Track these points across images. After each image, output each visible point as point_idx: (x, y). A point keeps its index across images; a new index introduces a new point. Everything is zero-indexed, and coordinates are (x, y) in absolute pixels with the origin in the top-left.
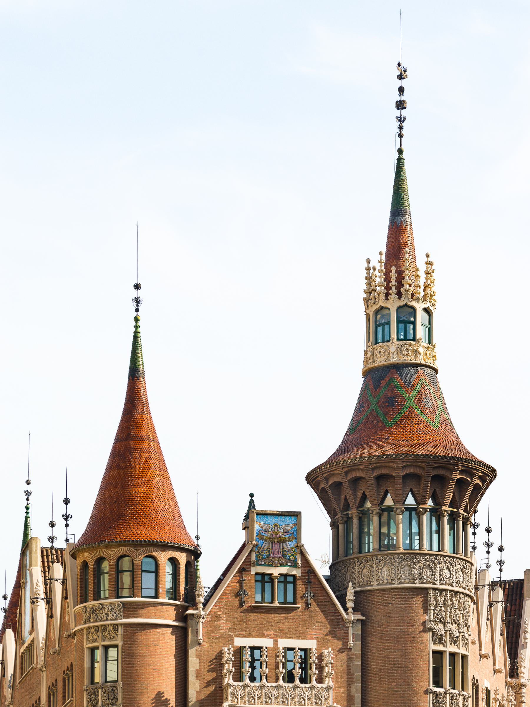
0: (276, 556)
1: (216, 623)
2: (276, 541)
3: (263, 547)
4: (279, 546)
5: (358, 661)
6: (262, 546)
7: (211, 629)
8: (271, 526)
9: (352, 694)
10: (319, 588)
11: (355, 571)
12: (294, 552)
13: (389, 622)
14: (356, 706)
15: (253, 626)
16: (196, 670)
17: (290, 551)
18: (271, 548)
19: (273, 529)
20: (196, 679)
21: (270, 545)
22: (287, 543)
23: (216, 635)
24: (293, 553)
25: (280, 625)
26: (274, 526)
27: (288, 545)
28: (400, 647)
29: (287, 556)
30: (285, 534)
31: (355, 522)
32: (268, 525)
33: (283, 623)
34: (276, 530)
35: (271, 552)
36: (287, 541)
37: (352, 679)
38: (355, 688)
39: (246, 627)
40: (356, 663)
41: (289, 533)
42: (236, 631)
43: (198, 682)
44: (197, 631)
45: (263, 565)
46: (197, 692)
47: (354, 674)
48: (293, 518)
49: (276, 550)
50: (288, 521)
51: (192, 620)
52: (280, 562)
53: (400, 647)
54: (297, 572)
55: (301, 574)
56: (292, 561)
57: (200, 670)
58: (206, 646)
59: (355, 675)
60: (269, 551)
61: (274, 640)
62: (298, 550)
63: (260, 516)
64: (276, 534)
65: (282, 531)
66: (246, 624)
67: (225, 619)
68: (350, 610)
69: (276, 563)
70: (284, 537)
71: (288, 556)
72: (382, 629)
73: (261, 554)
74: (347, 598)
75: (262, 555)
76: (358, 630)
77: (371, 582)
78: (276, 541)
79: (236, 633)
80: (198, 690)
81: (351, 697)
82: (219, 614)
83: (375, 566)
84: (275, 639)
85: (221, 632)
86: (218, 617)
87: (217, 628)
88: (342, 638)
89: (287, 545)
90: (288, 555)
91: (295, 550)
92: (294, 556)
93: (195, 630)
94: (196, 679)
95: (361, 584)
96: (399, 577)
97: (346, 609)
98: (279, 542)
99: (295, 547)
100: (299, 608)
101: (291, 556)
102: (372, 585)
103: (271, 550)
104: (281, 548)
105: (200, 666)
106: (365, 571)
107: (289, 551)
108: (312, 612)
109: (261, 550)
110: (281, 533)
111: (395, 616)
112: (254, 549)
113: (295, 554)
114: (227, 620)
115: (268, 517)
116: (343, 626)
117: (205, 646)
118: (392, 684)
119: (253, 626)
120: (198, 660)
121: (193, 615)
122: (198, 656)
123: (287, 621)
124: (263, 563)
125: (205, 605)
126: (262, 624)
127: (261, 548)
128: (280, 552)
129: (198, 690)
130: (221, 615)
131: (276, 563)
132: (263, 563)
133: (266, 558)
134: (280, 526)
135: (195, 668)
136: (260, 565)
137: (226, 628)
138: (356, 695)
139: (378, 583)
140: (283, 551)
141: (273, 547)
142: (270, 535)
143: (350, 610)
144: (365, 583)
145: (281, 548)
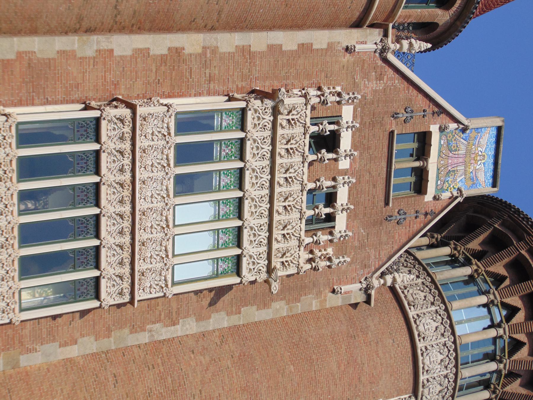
0: (450, 161)
1: (374, 73)
2: (467, 160)
3: (462, 140)
4: (461, 164)
5: (316, 306)
6: (462, 138)
7: (366, 65)
8: (484, 149)
9: (273, 304)
10: (409, 231)
11: (416, 280)
12: (453, 187)
13: (370, 344)
14: (256, 313)
15: (367, 135)
16: (312, 44)
17: (454, 181)
18: (460, 152)
19: (480, 153)
20: (299, 45)
21: (462, 152)
22: (463, 177)
23: (357, 75)
24: (451, 186)
25: (367, 177)
26: (484, 154)
27: (461, 178)
28: (342, 368)
29: (449, 177)
30: (474, 173)
31: (467, 271)
32: (485, 146)
33: (368, 182)
34: (478, 158)
35: (454, 153)
36: (465, 175)
37: (293, 300)
38: (280, 307)
39: (366, 123)
40: (314, 302)
41: (474, 178)
42: (361, 108)
43: (295, 48)
44: (363, 43)
45: (440, 142)
46: (281, 46)
47: (299, 301)
48: (491, 181)
49: (456, 161)
50: (488, 174)
51: (379, 34)
52: (442, 169)
53: (342, 368)
54: (429, 197)
55: (427, 202)
56: (443, 187)
57: (312, 50)
58: (344, 60)
59: (299, 304)
60: (456, 151)
61: (347, 169)
62: (455, 194)
63: (495, 132)
64: (474, 158)
65: (478, 167)
66: (369, 123)
67: (378, 88)
68: (382, 281)
69: (442, 162)
70: (471, 170)
71: (449, 179)
72: (360, 334)
73: (453, 138)
74: (396, 275)
75: (451, 140)
76: (356, 297)
77: (414, 306)
78: (467, 160)
79: (359, 107)
80: (284, 48)
81: (268, 303)
82: (384, 79)
83: (433, 308)
84: (349, 170)
85: (361, 82)
86: (380, 78)
87: (366, 76)
88: (346, 276)
89: (461, 175)
90: (450, 179)
91: (454, 188)
92: (448, 188)
93: (366, 40)
94: (299, 45)
95: (406, 291)
96: (428, 347)
97: (383, 275)
98: (465, 163)
99: (458, 188)
100: (387, 203)
101: (448, 183)
102: (410, 309)
103: (457, 152)
104: (458, 168)
105: (318, 50)
106: (423, 294)
107: (454, 180)
108: (381, 224)
109: (457, 137)
110: (475, 165)
111: (380, 352)
112: (461, 126)
113: (451, 189)
114: (376, 91)
115: (494, 146)
116: (362, 275)
117: (344, 58)
118: (292, 366)
119: (367, 135)
120: (325, 46)
121: (386, 35)
122: (331, 46)
123: (371, 186)
124: (442, 142)
125: (398, 54)
126: (369, 148)
127: (460, 137)
128: (453, 166)
129: (284, 48)
130: (383, 81)
131: (442, 162)
132: (442, 142)
133: (448, 144)
134: (484, 163)
135: (315, 43)
136: (441, 139)
137: (366, 91)
138: (270, 311)
139: (416, 317)
140: (454, 171)
141: (459, 156)
142: (474, 149)
143: (382, 281)
144: (411, 299)
145: (458, 168)
